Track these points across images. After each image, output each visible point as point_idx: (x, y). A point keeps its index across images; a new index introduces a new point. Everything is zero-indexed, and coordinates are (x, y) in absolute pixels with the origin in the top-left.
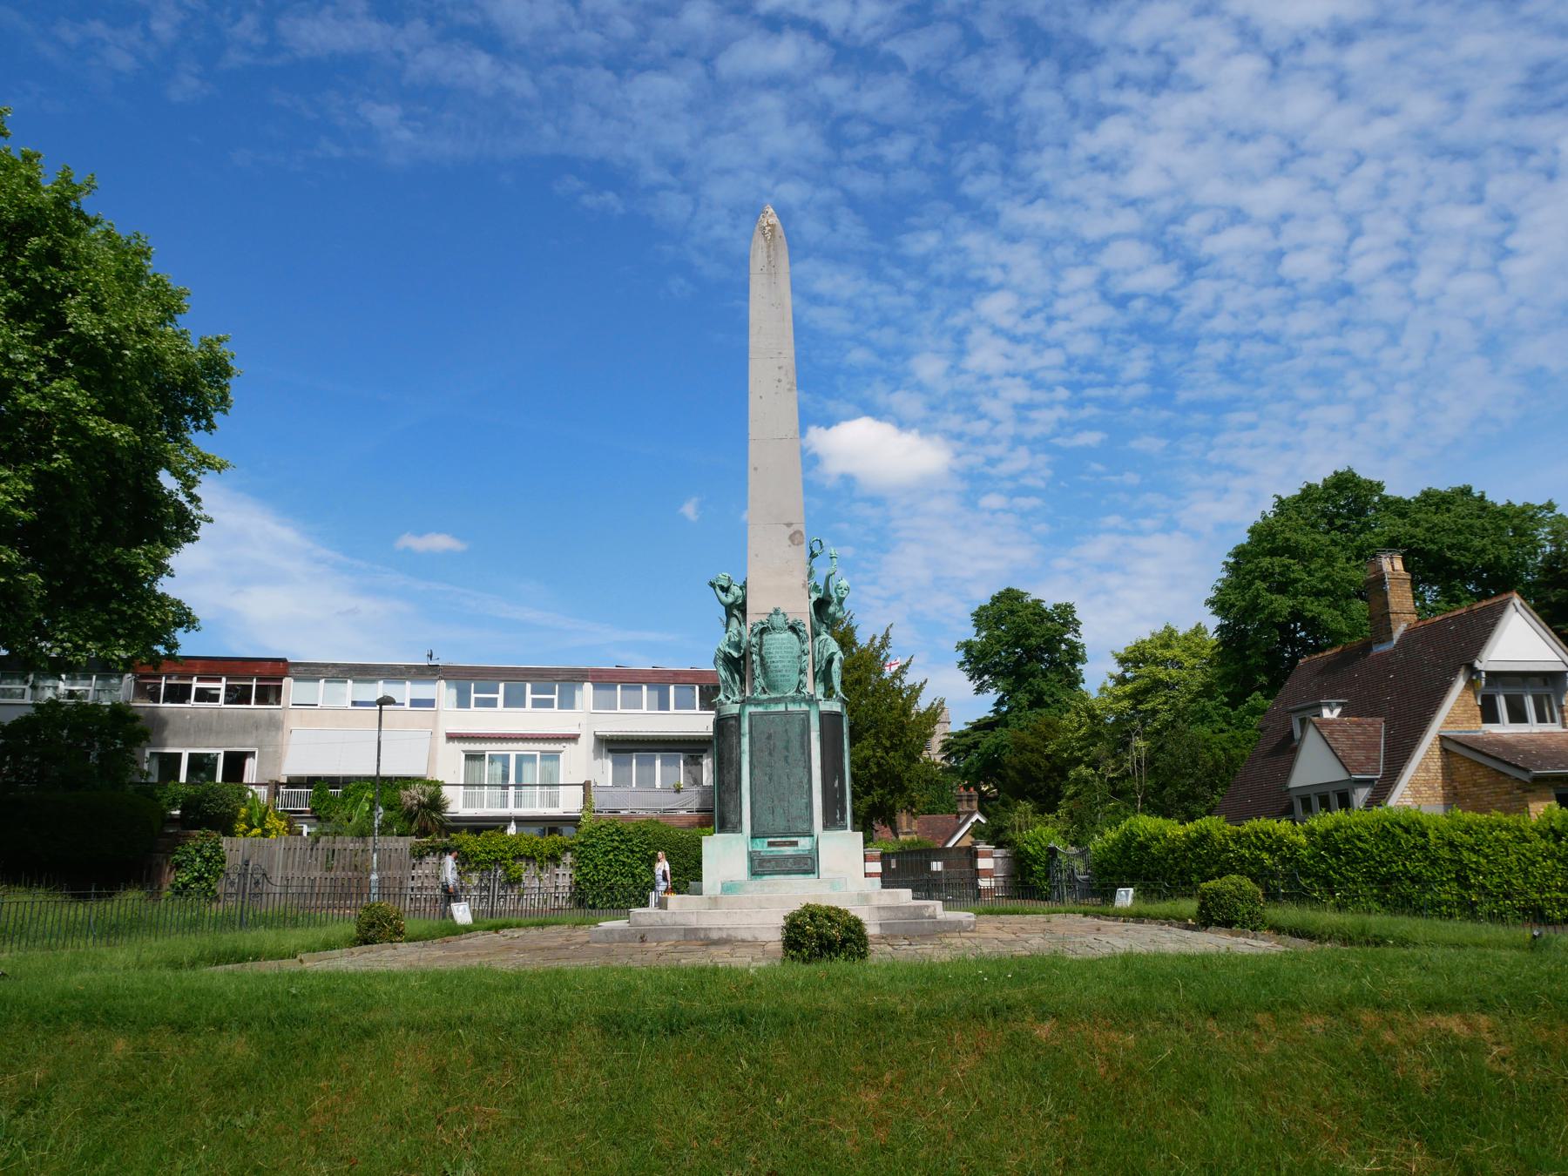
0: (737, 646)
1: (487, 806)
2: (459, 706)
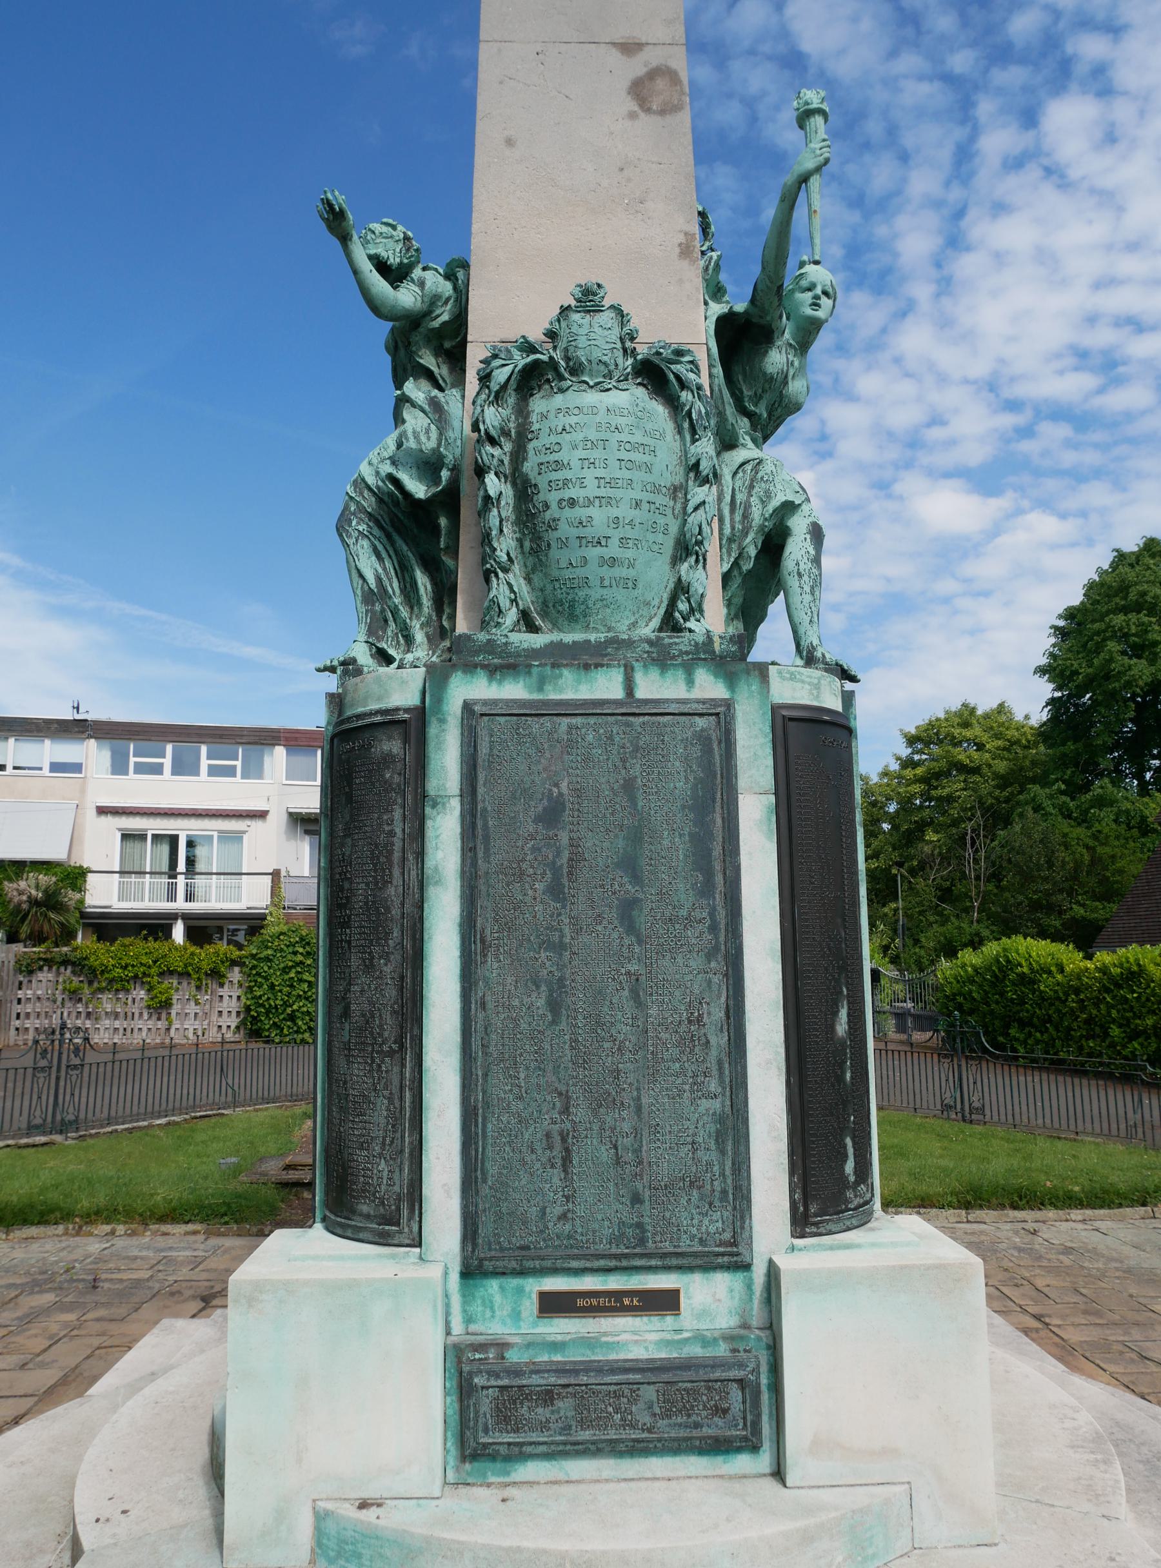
0: (429, 466)
1: (148, 898)
2: (113, 774)
